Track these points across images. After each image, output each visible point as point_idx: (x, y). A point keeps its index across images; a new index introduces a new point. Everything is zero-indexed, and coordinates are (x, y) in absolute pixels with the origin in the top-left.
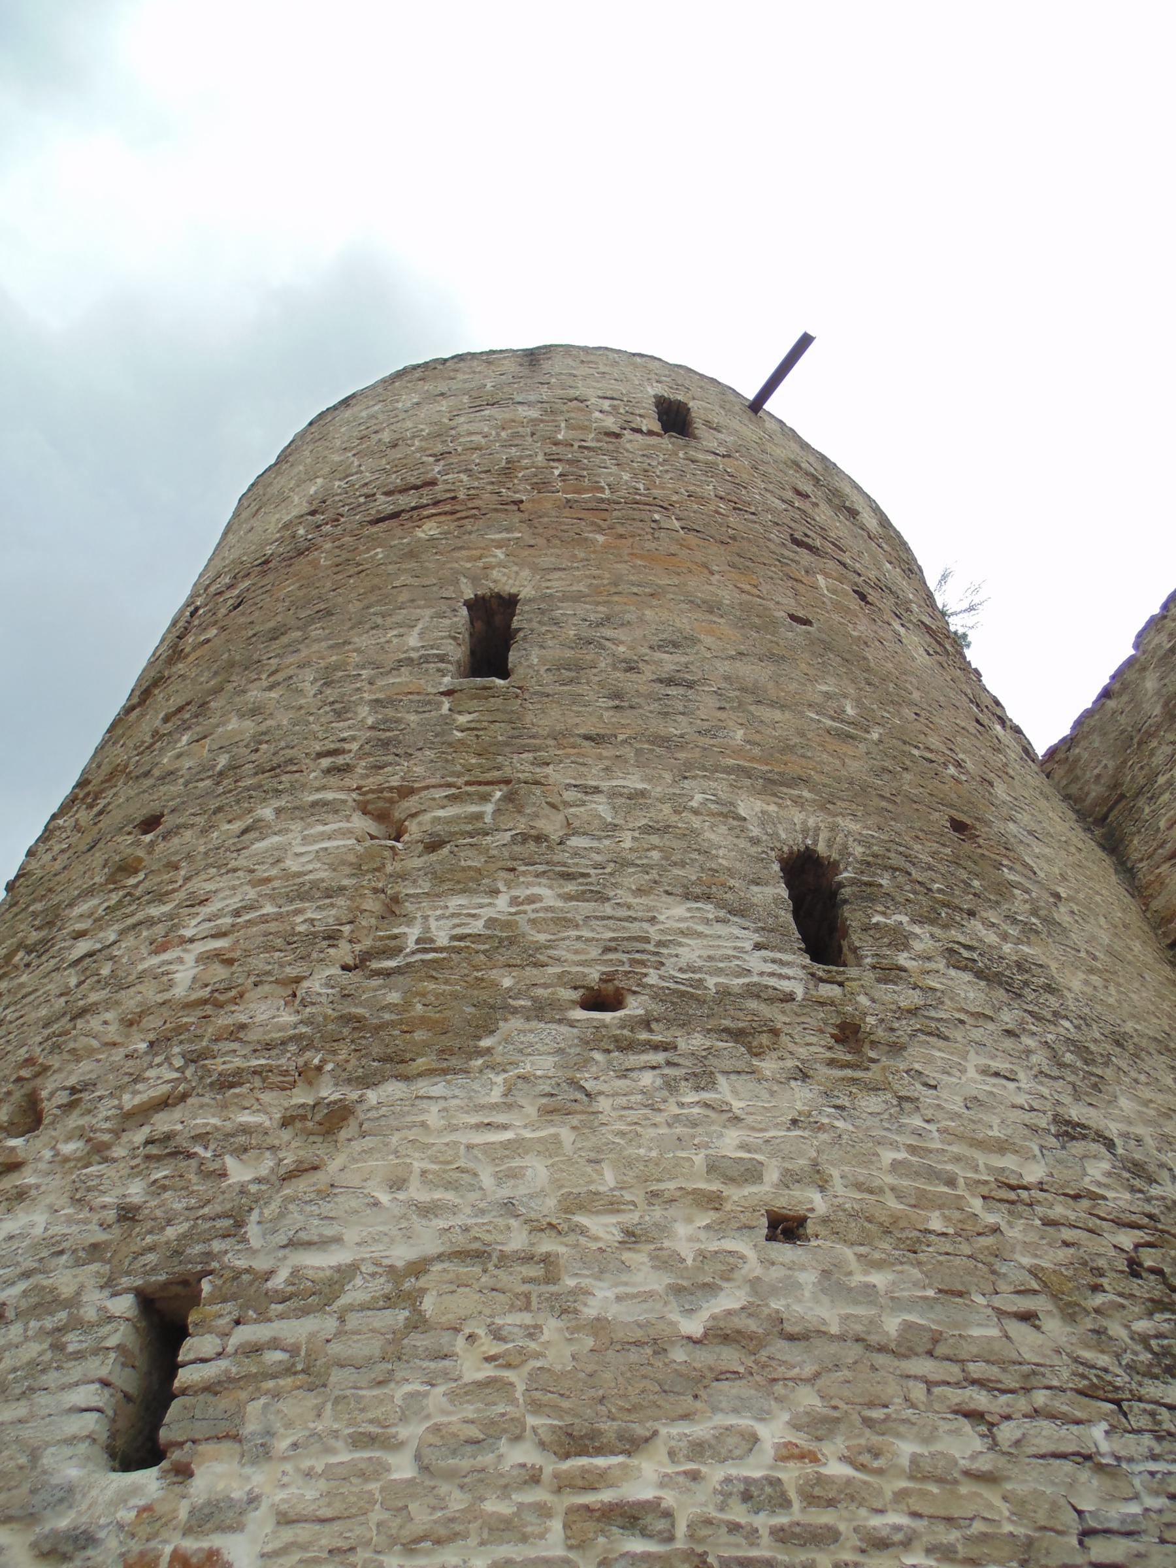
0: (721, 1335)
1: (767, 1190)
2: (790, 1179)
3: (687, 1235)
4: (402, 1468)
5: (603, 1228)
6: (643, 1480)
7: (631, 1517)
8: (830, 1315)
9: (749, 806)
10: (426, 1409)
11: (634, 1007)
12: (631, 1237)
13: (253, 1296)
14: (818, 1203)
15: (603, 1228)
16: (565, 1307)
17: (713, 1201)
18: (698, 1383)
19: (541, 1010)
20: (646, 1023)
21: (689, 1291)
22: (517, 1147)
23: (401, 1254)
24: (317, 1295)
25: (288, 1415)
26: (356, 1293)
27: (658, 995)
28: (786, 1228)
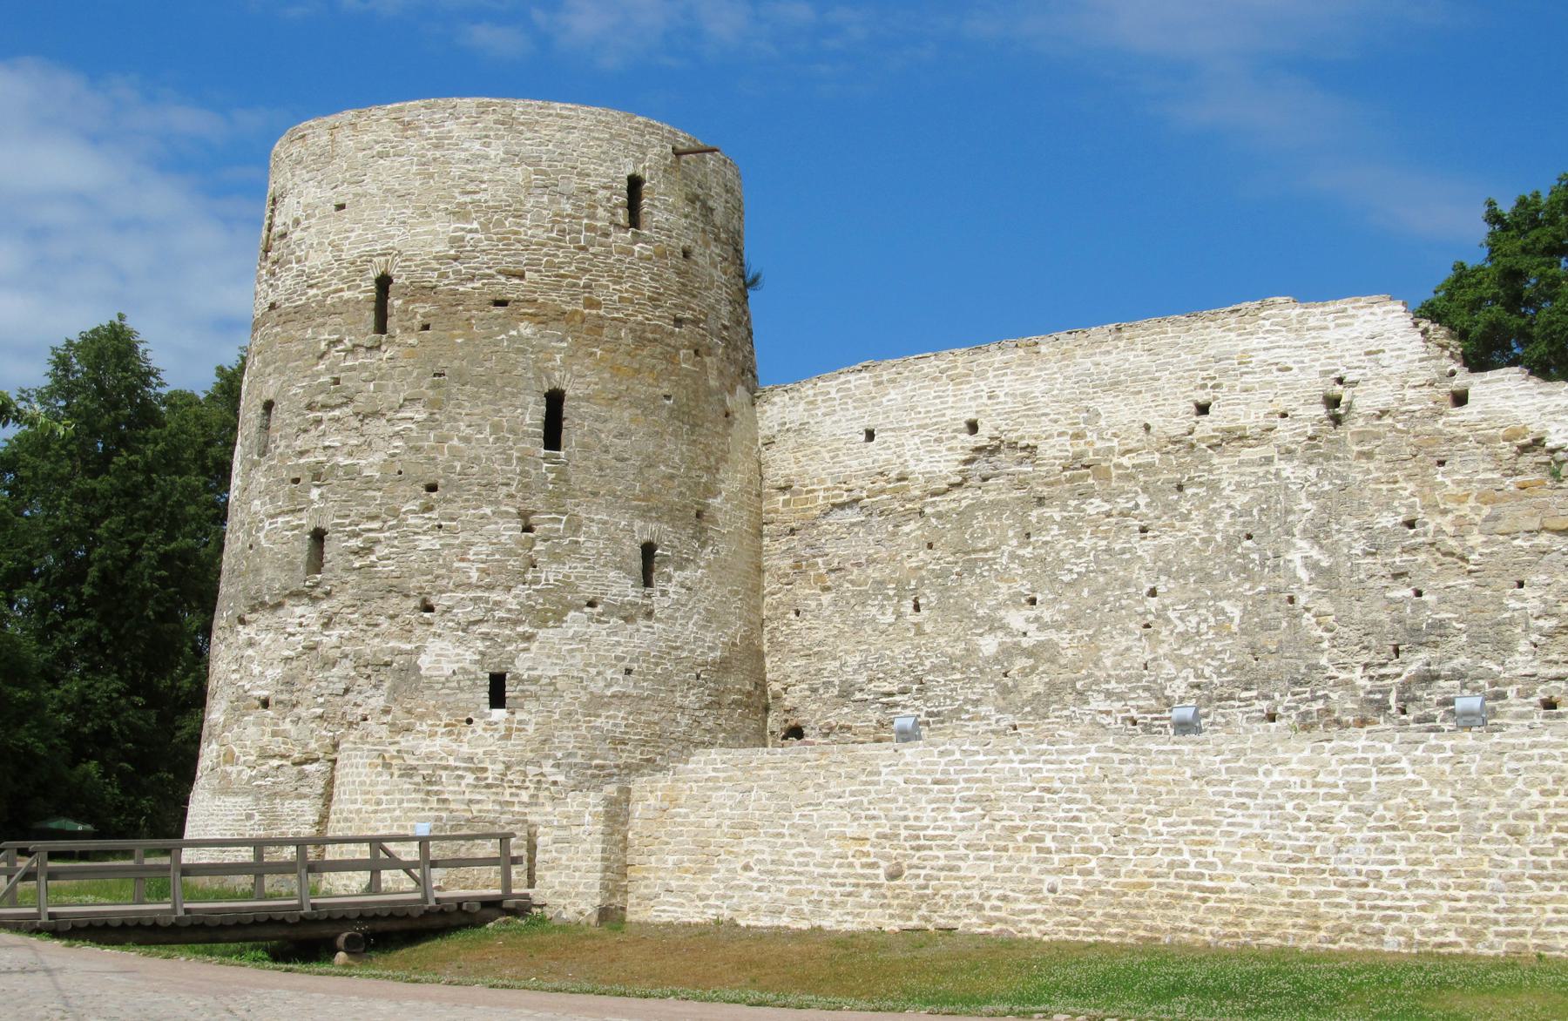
0: (613, 696)
1: (626, 663)
2: (632, 660)
3: (609, 674)
4: (556, 717)
5: (593, 671)
6: (598, 722)
7: (595, 728)
8: (634, 692)
9: (638, 524)
10: (559, 707)
11: (599, 609)
12: (599, 673)
13: (517, 678)
14: (635, 666)
15: (593, 671)
16: (585, 688)
17: (612, 666)
18: (610, 704)
19: (579, 608)
20: (602, 614)
21: (609, 686)
22: (573, 650)
23: (551, 674)
24: (535, 681)
25: (531, 705)
26: (544, 681)
27: (607, 605)
28: (628, 672)
